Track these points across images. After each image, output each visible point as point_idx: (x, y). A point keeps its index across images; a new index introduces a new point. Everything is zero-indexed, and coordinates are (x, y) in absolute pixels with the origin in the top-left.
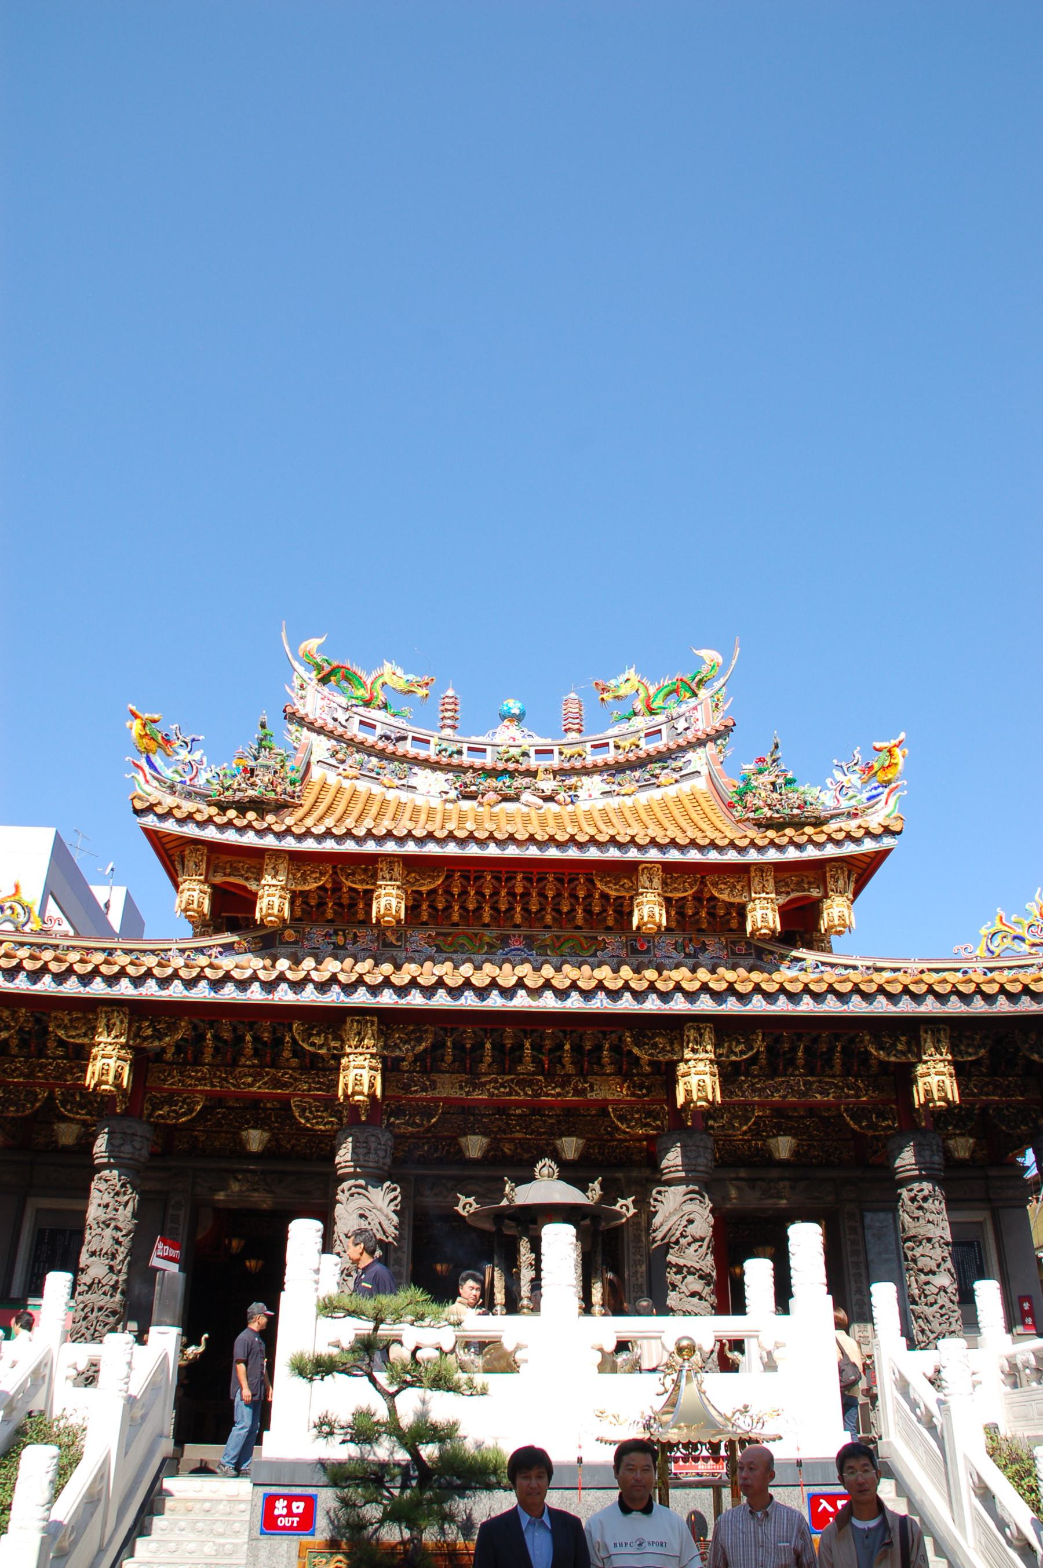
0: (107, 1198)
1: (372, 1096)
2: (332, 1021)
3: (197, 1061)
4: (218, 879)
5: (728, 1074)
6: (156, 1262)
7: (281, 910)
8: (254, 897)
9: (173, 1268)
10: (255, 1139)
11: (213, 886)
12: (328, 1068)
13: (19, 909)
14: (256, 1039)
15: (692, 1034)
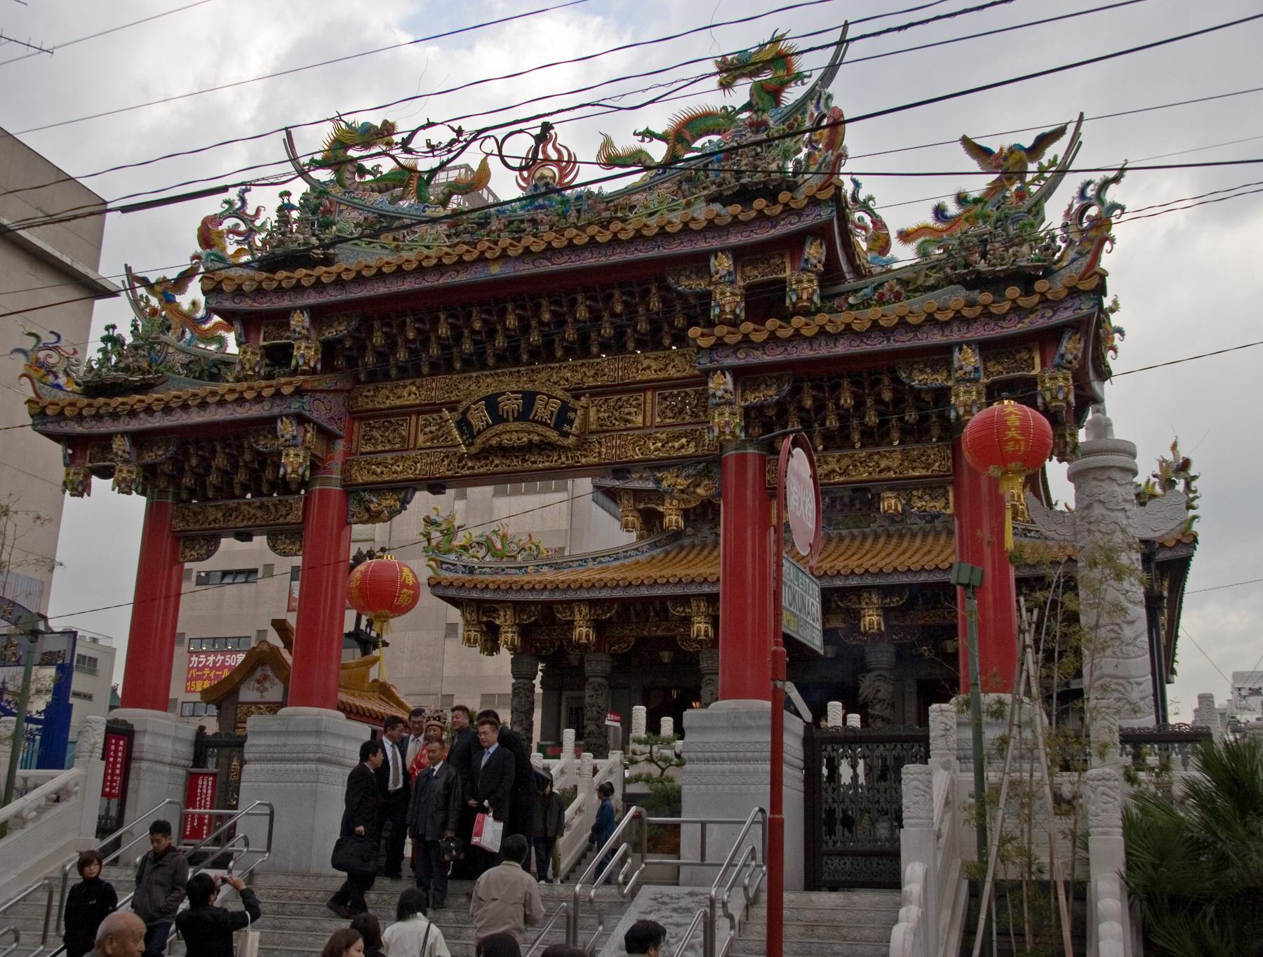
0: (592, 693)
1: (707, 635)
2: (684, 600)
3: (629, 621)
4: (642, 506)
5: (886, 612)
6: (607, 723)
7: (677, 522)
8: (661, 516)
9: (618, 724)
10: (666, 656)
11: (638, 510)
12: (687, 621)
13: (534, 548)
14: (655, 609)
15: (865, 595)
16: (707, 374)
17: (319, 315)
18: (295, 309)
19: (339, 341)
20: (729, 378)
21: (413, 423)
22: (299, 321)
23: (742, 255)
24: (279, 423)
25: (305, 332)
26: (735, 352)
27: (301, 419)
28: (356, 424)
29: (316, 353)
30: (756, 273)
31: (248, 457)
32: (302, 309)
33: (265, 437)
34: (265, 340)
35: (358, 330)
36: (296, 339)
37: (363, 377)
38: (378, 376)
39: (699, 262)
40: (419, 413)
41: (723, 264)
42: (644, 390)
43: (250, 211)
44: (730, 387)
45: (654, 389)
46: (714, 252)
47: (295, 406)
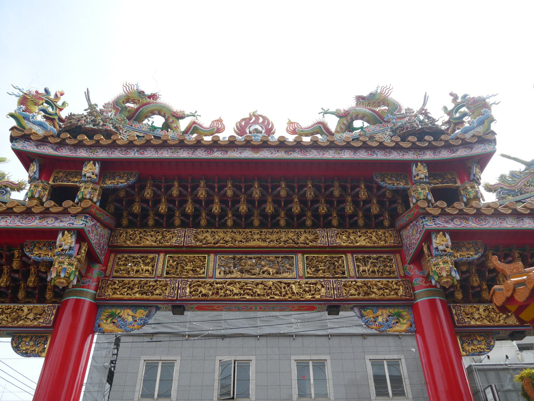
16: (428, 236)
17: (108, 167)
18: (89, 160)
19: (115, 190)
20: (448, 236)
21: (161, 260)
22: (91, 170)
23: (433, 167)
24: (60, 236)
25: (94, 177)
26: (452, 220)
27: (81, 236)
28: (113, 255)
29: (99, 195)
30: (436, 181)
31: (15, 265)
32: (95, 161)
33: (40, 249)
34: (53, 181)
35: (132, 187)
36: (85, 182)
37: (125, 222)
38: (139, 222)
39: (403, 169)
40: (166, 252)
41: (421, 172)
42: (345, 253)
43: (60, 103)
44: (450, 244)
45: (352, 253)
46: (416, 162)
47: (79, 223)
